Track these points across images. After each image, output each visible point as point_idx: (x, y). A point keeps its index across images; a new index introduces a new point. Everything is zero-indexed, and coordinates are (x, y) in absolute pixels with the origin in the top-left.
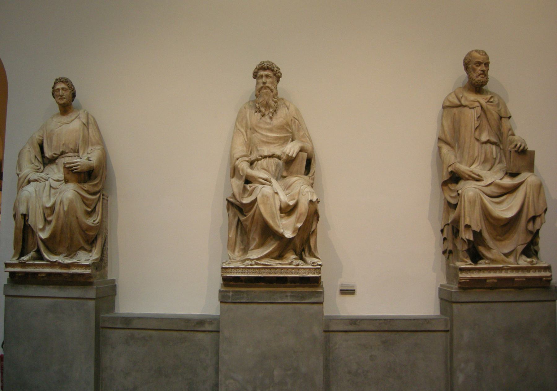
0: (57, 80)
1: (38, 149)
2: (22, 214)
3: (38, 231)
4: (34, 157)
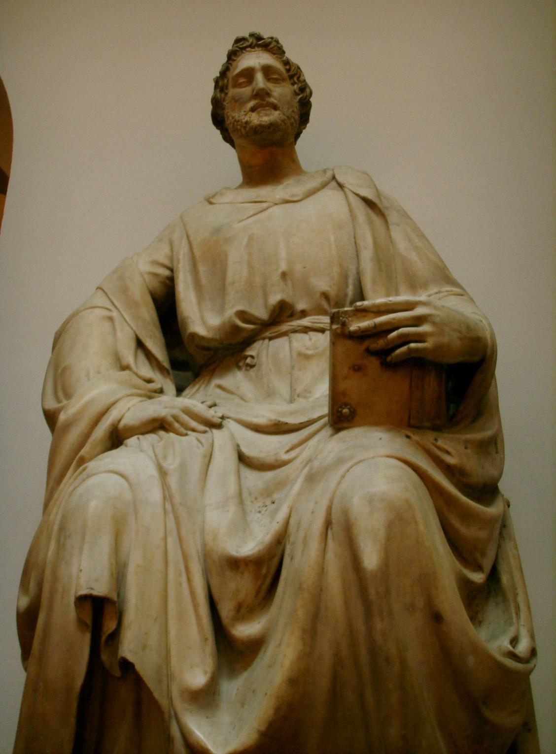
0: (238, 41)
1: (149, 312)
2: (82, 600)
3: (180, 705)
4: (132, 344)
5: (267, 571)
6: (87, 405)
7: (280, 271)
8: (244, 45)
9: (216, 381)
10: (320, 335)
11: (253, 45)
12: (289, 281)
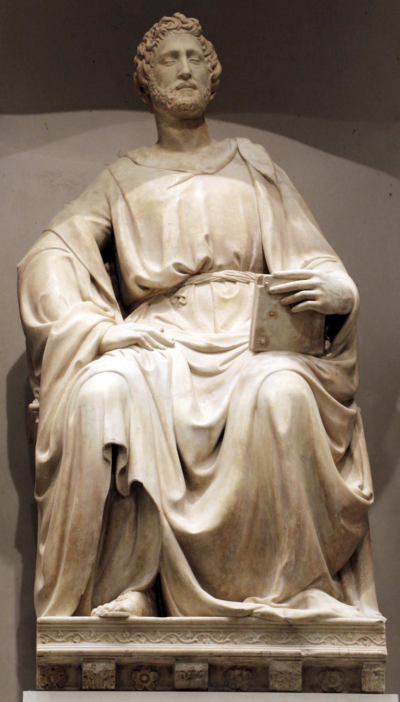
5: (216, 435)
6: (74, 327)
7: (204, 234)
8: (171, 27)
9: (154, 314)
10: (232, 284)
11: (178, 28)
12: (211, 243)
